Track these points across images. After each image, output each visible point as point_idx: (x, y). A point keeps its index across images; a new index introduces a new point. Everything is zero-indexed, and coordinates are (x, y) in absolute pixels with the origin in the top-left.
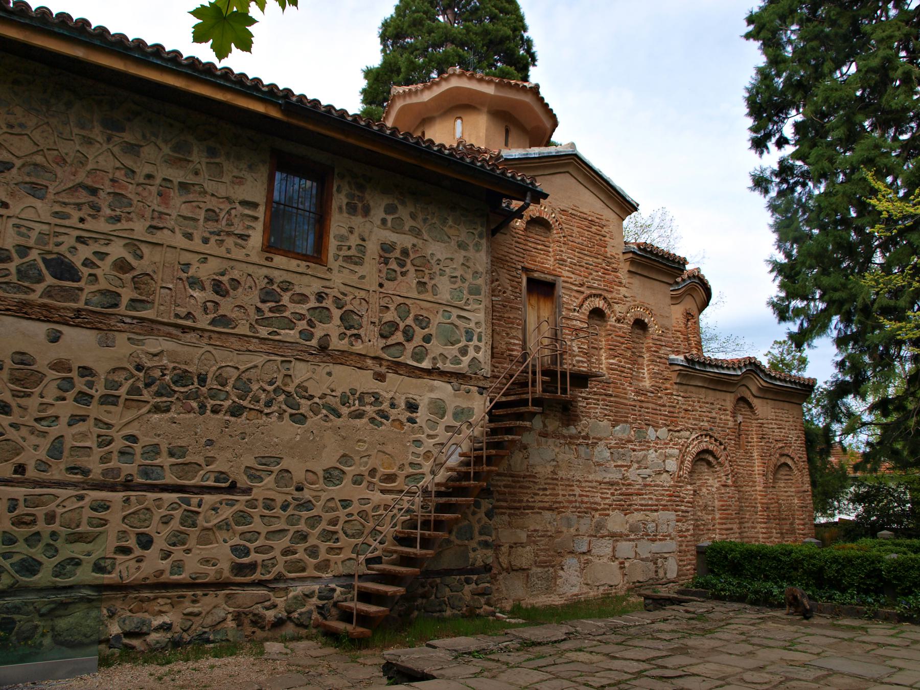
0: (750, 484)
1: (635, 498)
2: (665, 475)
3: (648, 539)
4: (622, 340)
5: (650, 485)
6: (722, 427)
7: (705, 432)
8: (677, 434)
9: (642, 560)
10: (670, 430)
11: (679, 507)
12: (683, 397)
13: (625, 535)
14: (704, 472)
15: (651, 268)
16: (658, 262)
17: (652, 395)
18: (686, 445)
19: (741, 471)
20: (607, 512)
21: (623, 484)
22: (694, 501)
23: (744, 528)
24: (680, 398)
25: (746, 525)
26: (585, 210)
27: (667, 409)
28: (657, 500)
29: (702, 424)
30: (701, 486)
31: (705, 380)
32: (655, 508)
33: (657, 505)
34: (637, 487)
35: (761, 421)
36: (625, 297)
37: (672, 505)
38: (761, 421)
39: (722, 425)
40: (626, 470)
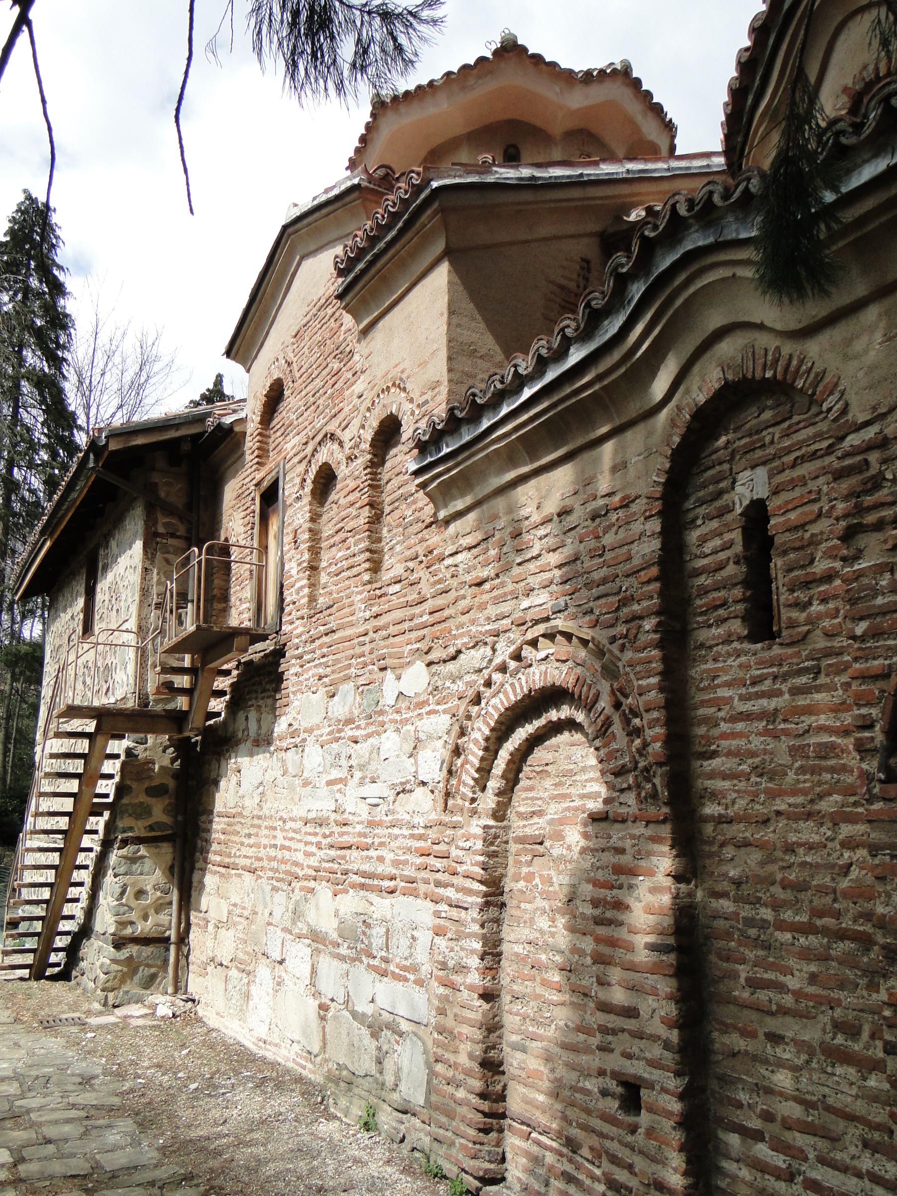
0: (827, 805)
1: (354, 854)
2: (420, 791)
3: (369, 965)
4: (351, 498)
5: (379, 824)
6: (604, 581)
7: (541, 628)
8: (451, 667)
9: (354, 1014)
10: (429, 664)
11: (441, 891)
12: (470, 549)
13: (332, 943)
14: (584, 770)
15: (386, 282)
16: (377, 257)
17: (397, 587)
18: (471, 693)
19: (756, 742)
20: (312, 884)
21: (337, 823)
22: (529, 878)
23: (775, 1039)
24: (460, 558)
25: (790, 1028)
26: (321, 293)
27: (428, 606)
28: (396, 863)
29: (525, 604)
30: (561, 822)
31: (510, 457)
32: (387, 884)
33: (392, 878)
34: (359, 828)
35: (870, 433)
36: (360, 397)
37: (427, 882)
38: (870, 433)
39: (604, 572)
40: (340, 791)
